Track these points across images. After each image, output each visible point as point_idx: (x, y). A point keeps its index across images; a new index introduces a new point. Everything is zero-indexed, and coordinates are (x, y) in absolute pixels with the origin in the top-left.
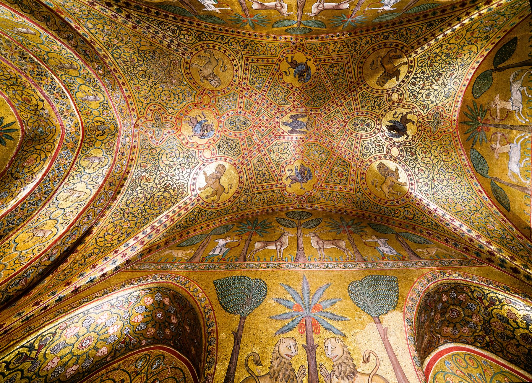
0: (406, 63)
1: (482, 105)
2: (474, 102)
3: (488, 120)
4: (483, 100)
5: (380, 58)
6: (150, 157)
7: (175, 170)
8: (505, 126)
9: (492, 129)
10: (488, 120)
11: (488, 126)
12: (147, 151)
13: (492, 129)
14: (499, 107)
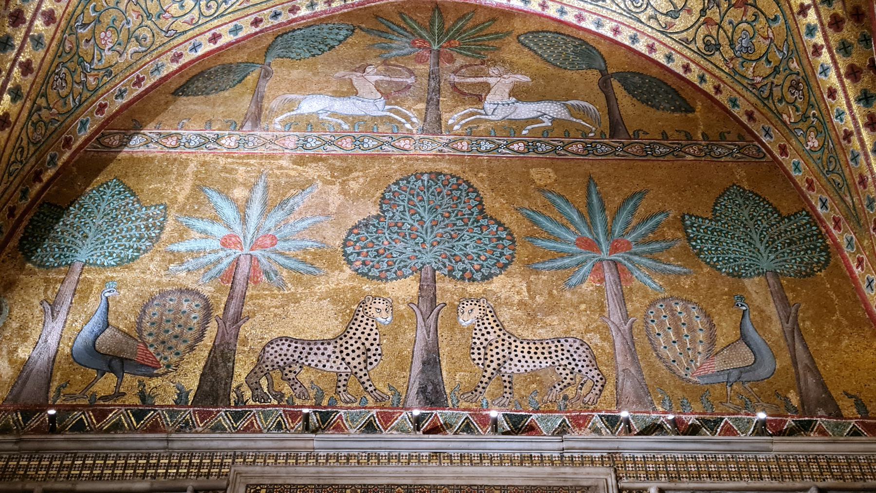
1: (498, 49)
2: (509, 33)
3: (451, 60)
4: (511, 50)
9: (423, 68)
10: (451, 60)
11: (432, 61)
13: (423, 68)
14: (491, 80)
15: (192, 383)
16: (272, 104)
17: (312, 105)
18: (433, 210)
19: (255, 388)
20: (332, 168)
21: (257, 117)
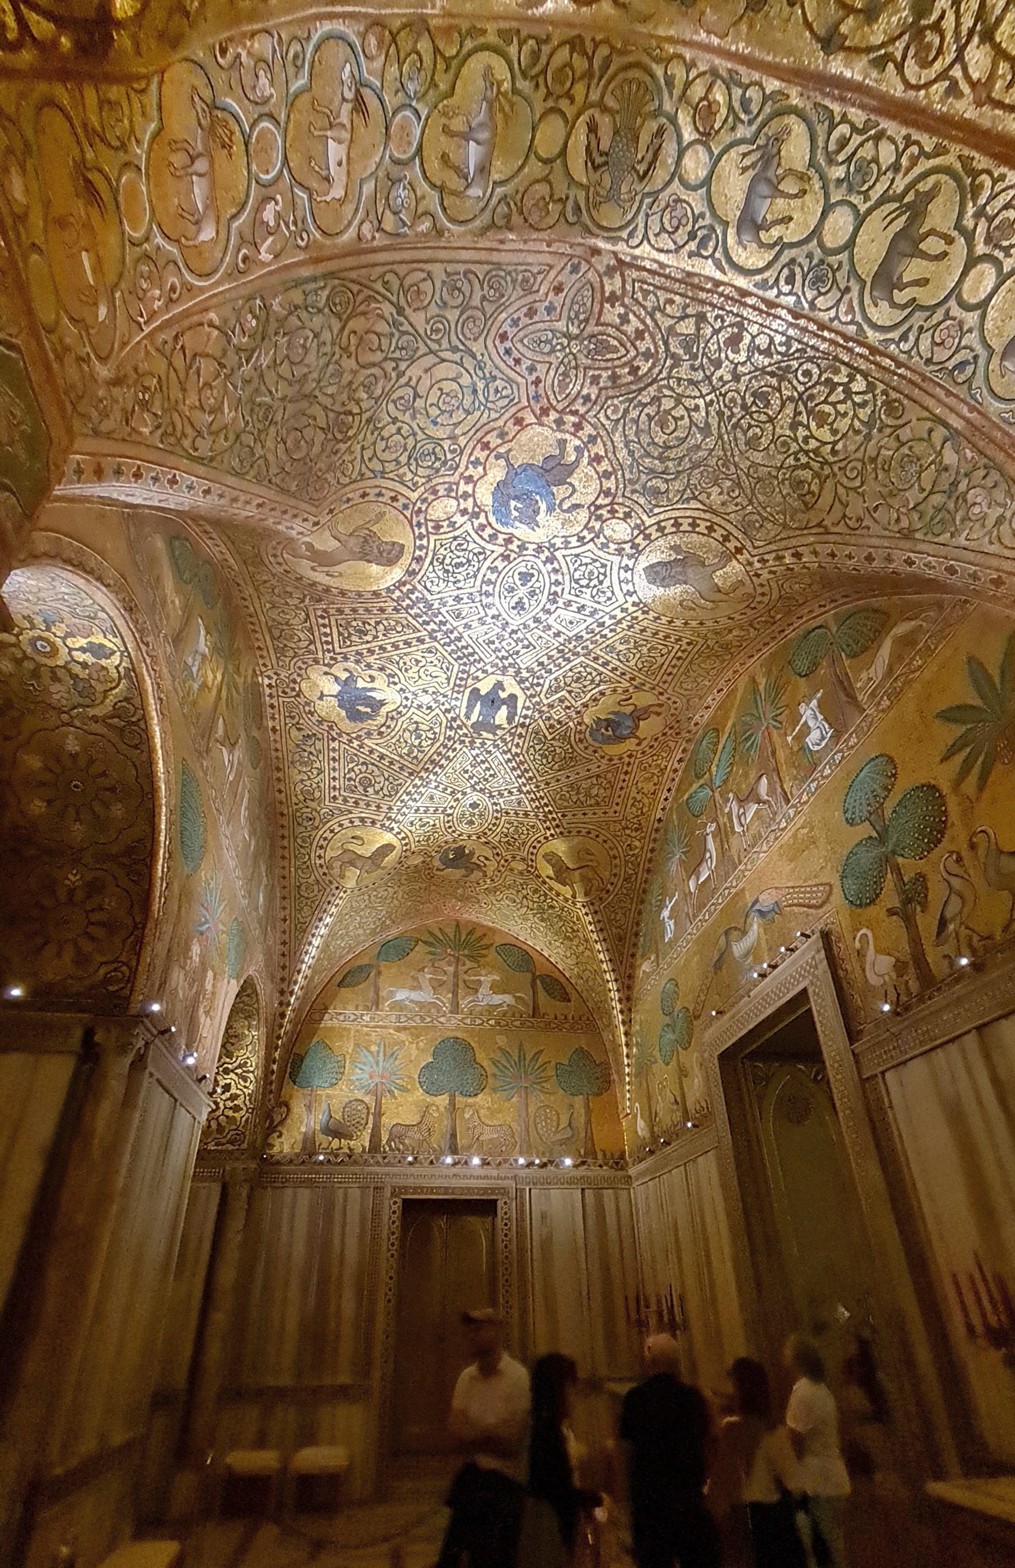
0: (574, 896)
5: (595, 864)
6: (452, 315)
7: (395, 420)
8: (456, 985)
12: (476, 301)
15: (367, 1144)
16: (383, 993)
17: (401, 995)
18: (454, 1059)
19: (390, 1146)
20: (412, 1034)
21: (377, 1003)
